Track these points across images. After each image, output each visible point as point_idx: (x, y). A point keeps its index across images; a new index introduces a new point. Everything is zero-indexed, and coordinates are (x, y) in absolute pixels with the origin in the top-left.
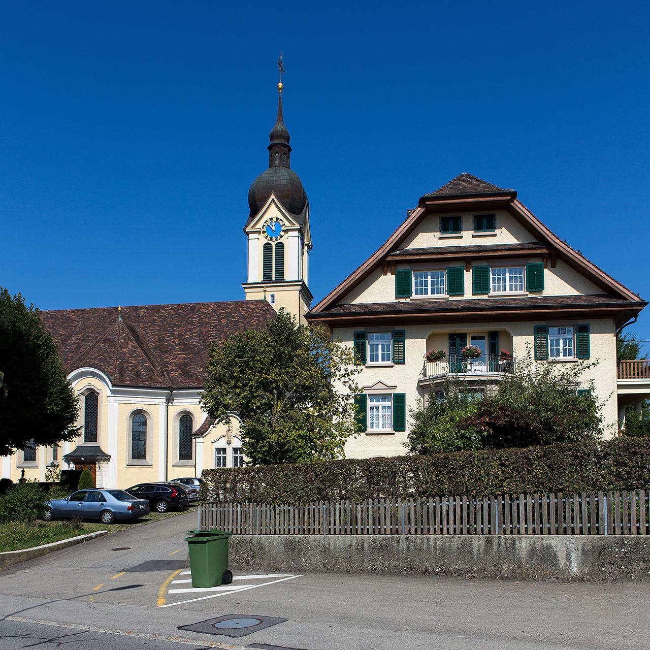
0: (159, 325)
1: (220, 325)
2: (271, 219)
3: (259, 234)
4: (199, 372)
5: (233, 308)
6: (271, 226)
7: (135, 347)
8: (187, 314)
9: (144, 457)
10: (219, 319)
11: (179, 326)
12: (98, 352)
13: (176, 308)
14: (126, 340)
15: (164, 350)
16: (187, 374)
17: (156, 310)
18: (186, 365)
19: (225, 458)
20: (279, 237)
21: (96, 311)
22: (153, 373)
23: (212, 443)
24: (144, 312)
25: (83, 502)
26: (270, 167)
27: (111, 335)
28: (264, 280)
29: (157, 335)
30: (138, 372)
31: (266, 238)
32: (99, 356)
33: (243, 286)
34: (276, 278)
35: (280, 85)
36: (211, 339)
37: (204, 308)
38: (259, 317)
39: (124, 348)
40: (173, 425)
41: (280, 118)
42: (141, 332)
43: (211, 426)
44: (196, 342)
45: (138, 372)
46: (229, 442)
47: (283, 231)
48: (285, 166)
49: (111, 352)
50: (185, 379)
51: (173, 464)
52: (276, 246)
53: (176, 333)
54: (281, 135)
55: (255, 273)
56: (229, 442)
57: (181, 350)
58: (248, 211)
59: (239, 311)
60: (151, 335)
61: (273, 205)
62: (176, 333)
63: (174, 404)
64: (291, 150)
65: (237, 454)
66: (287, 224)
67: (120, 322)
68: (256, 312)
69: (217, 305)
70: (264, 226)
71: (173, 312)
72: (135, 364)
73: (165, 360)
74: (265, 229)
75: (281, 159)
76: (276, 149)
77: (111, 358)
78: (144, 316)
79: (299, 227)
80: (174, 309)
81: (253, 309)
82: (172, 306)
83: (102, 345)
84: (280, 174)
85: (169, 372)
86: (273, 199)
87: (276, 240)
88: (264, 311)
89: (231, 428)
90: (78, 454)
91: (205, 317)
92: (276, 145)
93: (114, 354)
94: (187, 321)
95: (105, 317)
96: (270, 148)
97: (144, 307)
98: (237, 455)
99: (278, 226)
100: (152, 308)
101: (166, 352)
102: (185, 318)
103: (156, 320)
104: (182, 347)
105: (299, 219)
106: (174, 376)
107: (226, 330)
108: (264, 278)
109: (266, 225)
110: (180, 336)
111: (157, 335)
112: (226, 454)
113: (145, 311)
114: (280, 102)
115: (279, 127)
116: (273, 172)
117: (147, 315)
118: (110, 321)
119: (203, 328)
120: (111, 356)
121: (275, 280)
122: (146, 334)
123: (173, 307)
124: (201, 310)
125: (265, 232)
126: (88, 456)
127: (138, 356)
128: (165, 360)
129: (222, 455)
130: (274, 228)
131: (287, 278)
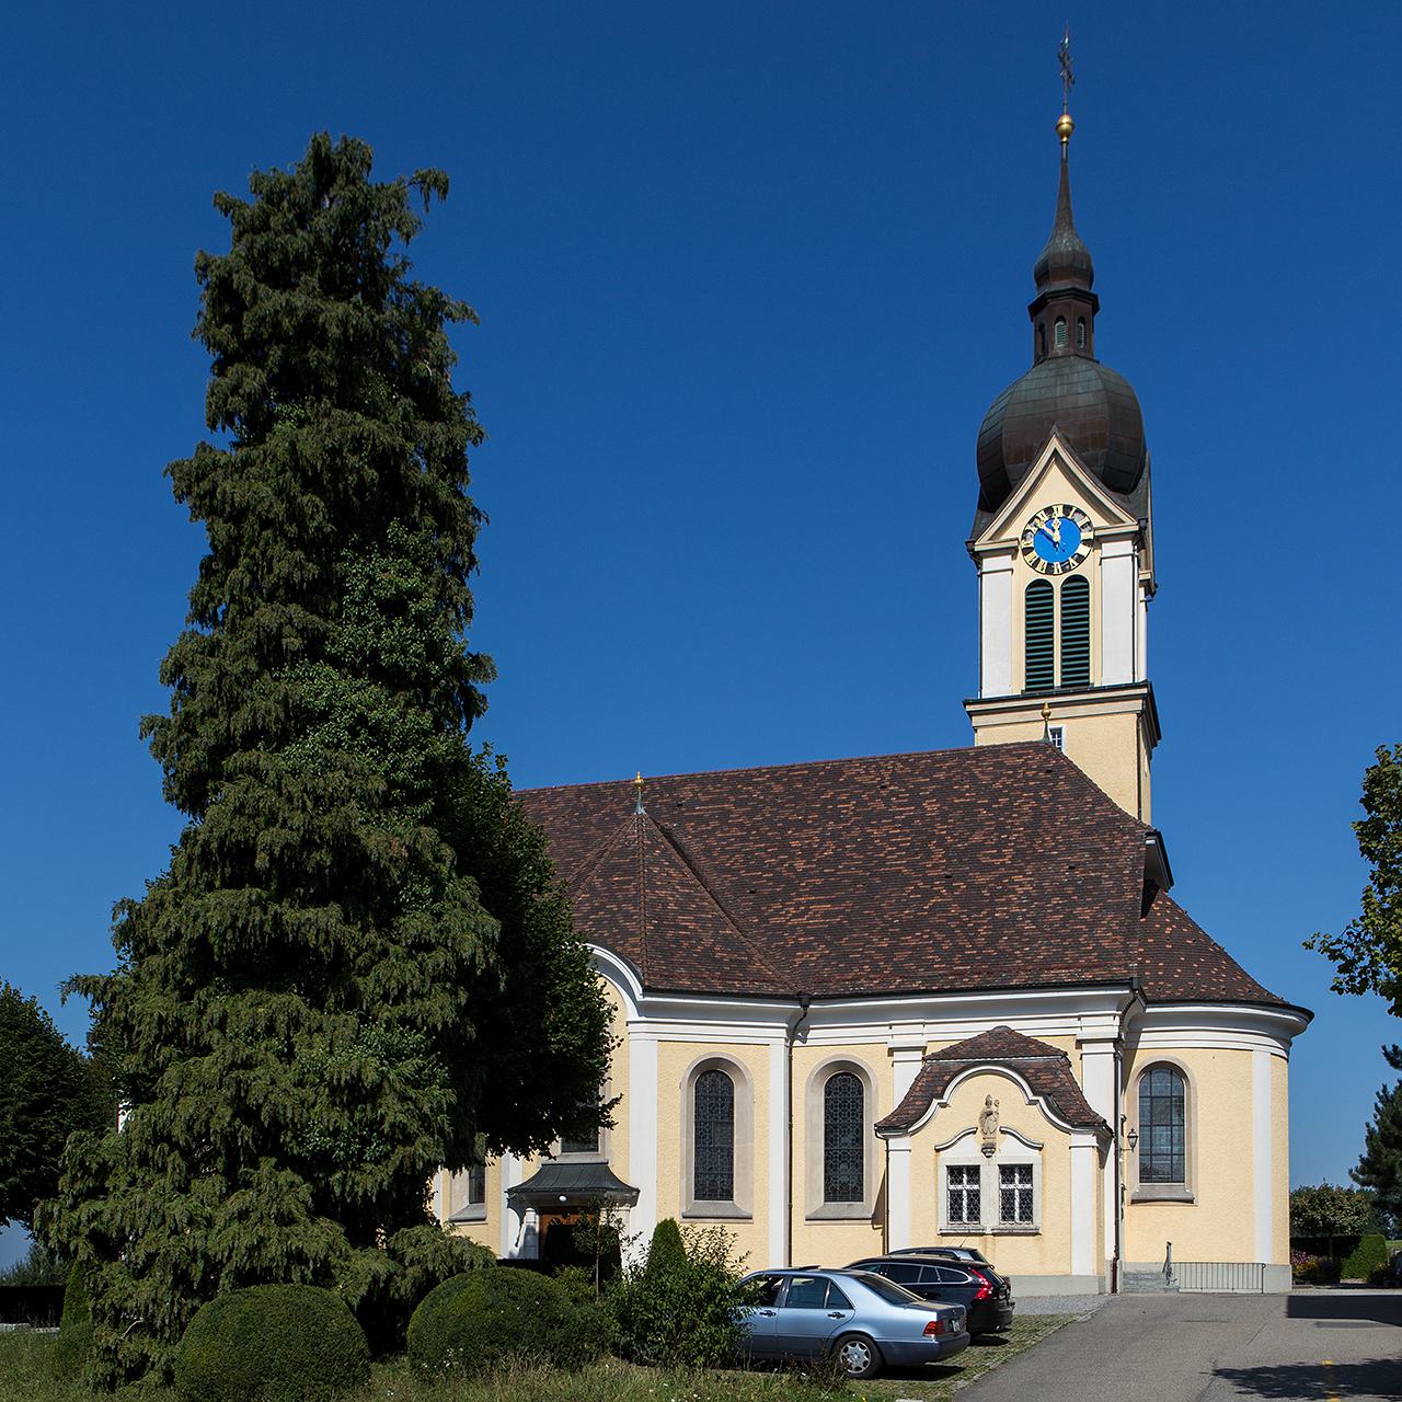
0: (741, 826)
1: (922, 817)
2: (1049, 510)
3: (1014, 557)
4: (879, 950)
5: (953, 767)
6: (1049, 531)
7: (689, 886)
8: (819, 793)
9: (728, 1194)
10: (916, 800)
11: (800, 826)
12: (588, 900)
13: (785, 776)
14: (662, 866)
15: (766, 891)
16: (844, 957)
17: (728, 784)
18: (837, 931)
19: (975, 1197)
20: (1072, 561)
21: (555, 793)
22: (748, 955)
23: (938, 1151)
24: (691, 790)
25: (773, 1310)
26: (1038, 361)
27: (621, 853)
28: (1027, 690)
29: (738, 851)
30: (708, 954)
31: (1034, 566)
32: (595, 910)
33: (969, 708)
34: (1063, 680)
35: (1065, 119)
36: (900, 857)
37: (868, 773)
38: (1036, 790)
39: (661, 888)
40: (806, 1105)
41: (1065, 217)
42: (694, 847)
43: (935, 1101)
44: (857, 867)
45: (708, 954)
46: (988, 1150)
47: (1087, 542)
48: (1082, 354)
49: (626, 900)
50: (842, 972)
51: (809, 1213)
52: (1063, 589)
53: (794, 844)
54: (1071, 266)
55: (1003, 669)
56: (988, 1150)
57: (815, 890)
58: (973, 487)
59: (973, 777)
60: (724, 852)
61: (1055, 470)
62: (794, 844)
63: (809, 1043)
64: (1098, 309)
65: (961, 1182)
66: (1098, 521)
67: (640, 817)
68: (1025, 777)
69: (904, 762)
70: (1026, 532)
71: (778, 789)
72: (695, 930)
73: (772, 921)
74: (1030, 542)
75: (1072, 338)
76: (1057, 306)
77: (628, 916)
78: (694, 802)
79: (1137, 528)
80: (778, 781)
81: (1015, 768)
82: (771, 771)
83: (598, 882)
84: (1075, 378)
85: (790, 953)
86: (1055, 450)
87: (1065, 571)
88: (1049, 772)
89: (993, 1108)
90: (548, 1184)
91: (872, 798)
92: (1056, 295)
93: (635, 906)
94: (822, 811)
95: (585, 811)
96: (1035, 309)
97: (692, 779)
98: (959, 1187)
99: (1070, 529)
100: (716, 779)
101: (773, 898)
102: (814, 802)
103: (730, 812)
104: (818, 882)
105: (1133, 506)
106: (806, 962)
107: (940, 829)
108: (1028, 683)
109: (1034, 529)
110: (808, 854)
111: (738, 851)
112: (978, 1182)
113: (697, 788)
114: (1064, 171)
115: (1065, 243)
116: (1053, 372)
117: (702, 798)
118: (601, 820)
119: (872, 826)
120: (628, 911)
121: (1063, 686)
122: (708, 851)
123: (774, 774)
124: (857, 779)
125: (1032, 549)
126: (575, 1190)
127: (701, 909)
128: (772, 921)
129: (965, 1187)
130: (1056, 537)
131: (1096, 679)
